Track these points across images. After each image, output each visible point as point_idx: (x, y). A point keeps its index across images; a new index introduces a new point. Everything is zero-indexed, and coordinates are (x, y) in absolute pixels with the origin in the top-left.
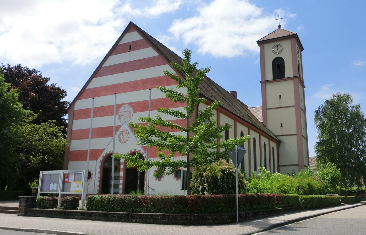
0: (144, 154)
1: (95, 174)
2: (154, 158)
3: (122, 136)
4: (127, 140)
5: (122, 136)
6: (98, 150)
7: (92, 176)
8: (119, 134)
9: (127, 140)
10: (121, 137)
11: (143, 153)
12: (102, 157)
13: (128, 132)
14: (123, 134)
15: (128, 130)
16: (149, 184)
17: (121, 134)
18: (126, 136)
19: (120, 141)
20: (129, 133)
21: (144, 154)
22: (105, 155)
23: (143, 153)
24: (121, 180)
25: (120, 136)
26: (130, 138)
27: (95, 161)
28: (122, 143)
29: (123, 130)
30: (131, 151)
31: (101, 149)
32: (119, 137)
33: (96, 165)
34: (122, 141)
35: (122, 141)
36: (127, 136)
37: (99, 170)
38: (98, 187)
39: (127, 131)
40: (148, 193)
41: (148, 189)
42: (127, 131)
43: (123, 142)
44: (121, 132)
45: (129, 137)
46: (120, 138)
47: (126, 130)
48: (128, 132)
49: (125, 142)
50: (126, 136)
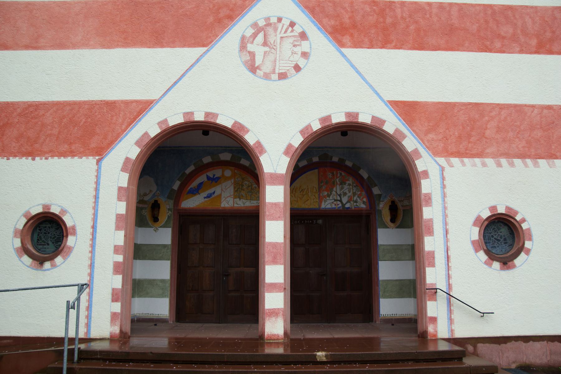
0: (404, 137)
1: (94, 227)
2: (466, 160)
3: (265, 44)
4: (297, 68)
5: (265, 44)
6: (111, 105)
7: (70, 241)
8: (243, 38)
9: (297, 68)
10: (256, 47)
11: (397, 130)
12: (137, 143)
13: (298, 29)
14: (271, 39)
15: (295, 20)
16: (450, 286)
17: (255, 35)
18: (287, 44)
19: (253, 69)
20: (303, 36)
21: (404, 137)
22: (154, 131)
23: (397, 130)
24: (274, 262)
25: (250, 47)
26: (311, 58)
27: (91, 161)
28: (267, 76)
29: (268, 19)
30: (328, 118)
31: (127, 103)
32: (243, 47)
33: (97, 183)
34: (267, 68)
35: (267, 68)
36: (296, 49)
37: (122, 208)
38: (114, 300)
39: (292, 24)
40: (452, 331)
41: (450, 311)
42: (292, 24)
43: (275, 77)
44: (258, 29)
45: (305, 55)
46: (252, 55)
47: (286, 22)
48: (298, 29)
49: (283, 76)
50: (288, 44)
